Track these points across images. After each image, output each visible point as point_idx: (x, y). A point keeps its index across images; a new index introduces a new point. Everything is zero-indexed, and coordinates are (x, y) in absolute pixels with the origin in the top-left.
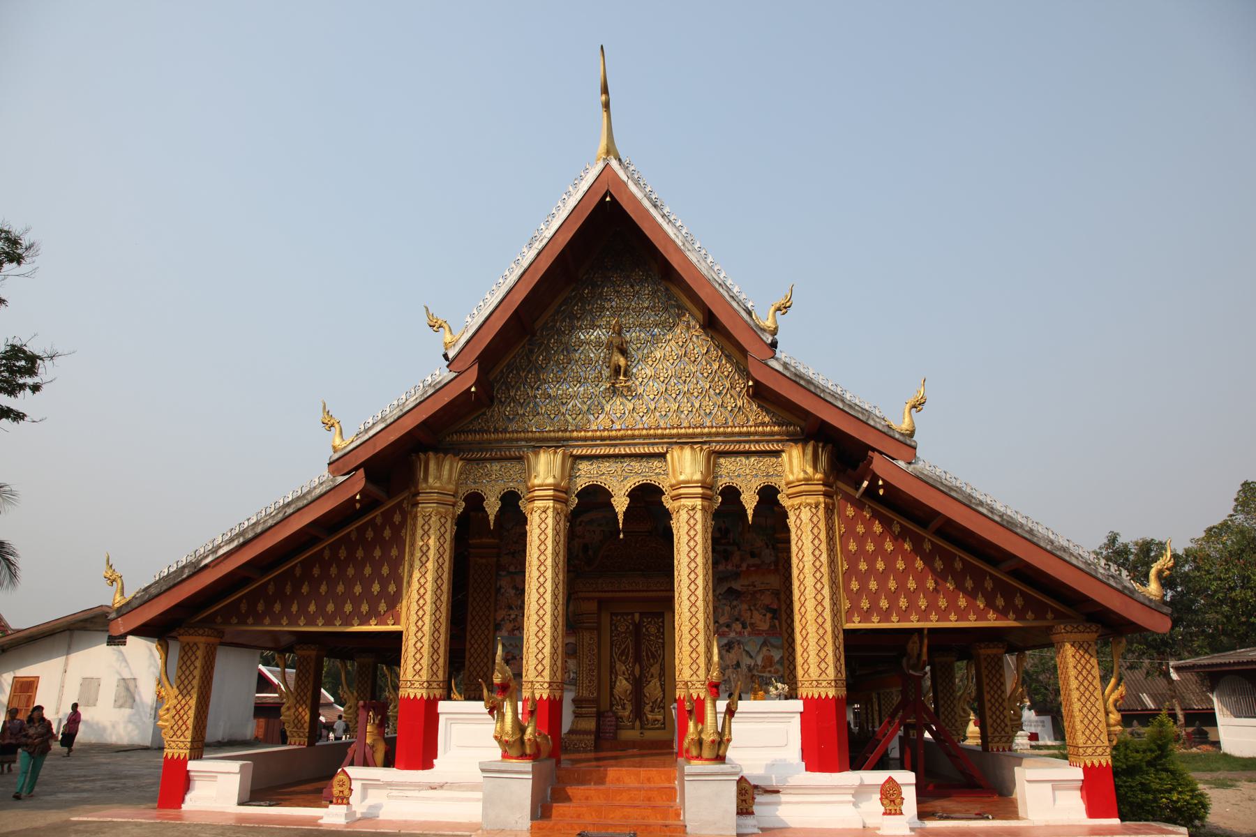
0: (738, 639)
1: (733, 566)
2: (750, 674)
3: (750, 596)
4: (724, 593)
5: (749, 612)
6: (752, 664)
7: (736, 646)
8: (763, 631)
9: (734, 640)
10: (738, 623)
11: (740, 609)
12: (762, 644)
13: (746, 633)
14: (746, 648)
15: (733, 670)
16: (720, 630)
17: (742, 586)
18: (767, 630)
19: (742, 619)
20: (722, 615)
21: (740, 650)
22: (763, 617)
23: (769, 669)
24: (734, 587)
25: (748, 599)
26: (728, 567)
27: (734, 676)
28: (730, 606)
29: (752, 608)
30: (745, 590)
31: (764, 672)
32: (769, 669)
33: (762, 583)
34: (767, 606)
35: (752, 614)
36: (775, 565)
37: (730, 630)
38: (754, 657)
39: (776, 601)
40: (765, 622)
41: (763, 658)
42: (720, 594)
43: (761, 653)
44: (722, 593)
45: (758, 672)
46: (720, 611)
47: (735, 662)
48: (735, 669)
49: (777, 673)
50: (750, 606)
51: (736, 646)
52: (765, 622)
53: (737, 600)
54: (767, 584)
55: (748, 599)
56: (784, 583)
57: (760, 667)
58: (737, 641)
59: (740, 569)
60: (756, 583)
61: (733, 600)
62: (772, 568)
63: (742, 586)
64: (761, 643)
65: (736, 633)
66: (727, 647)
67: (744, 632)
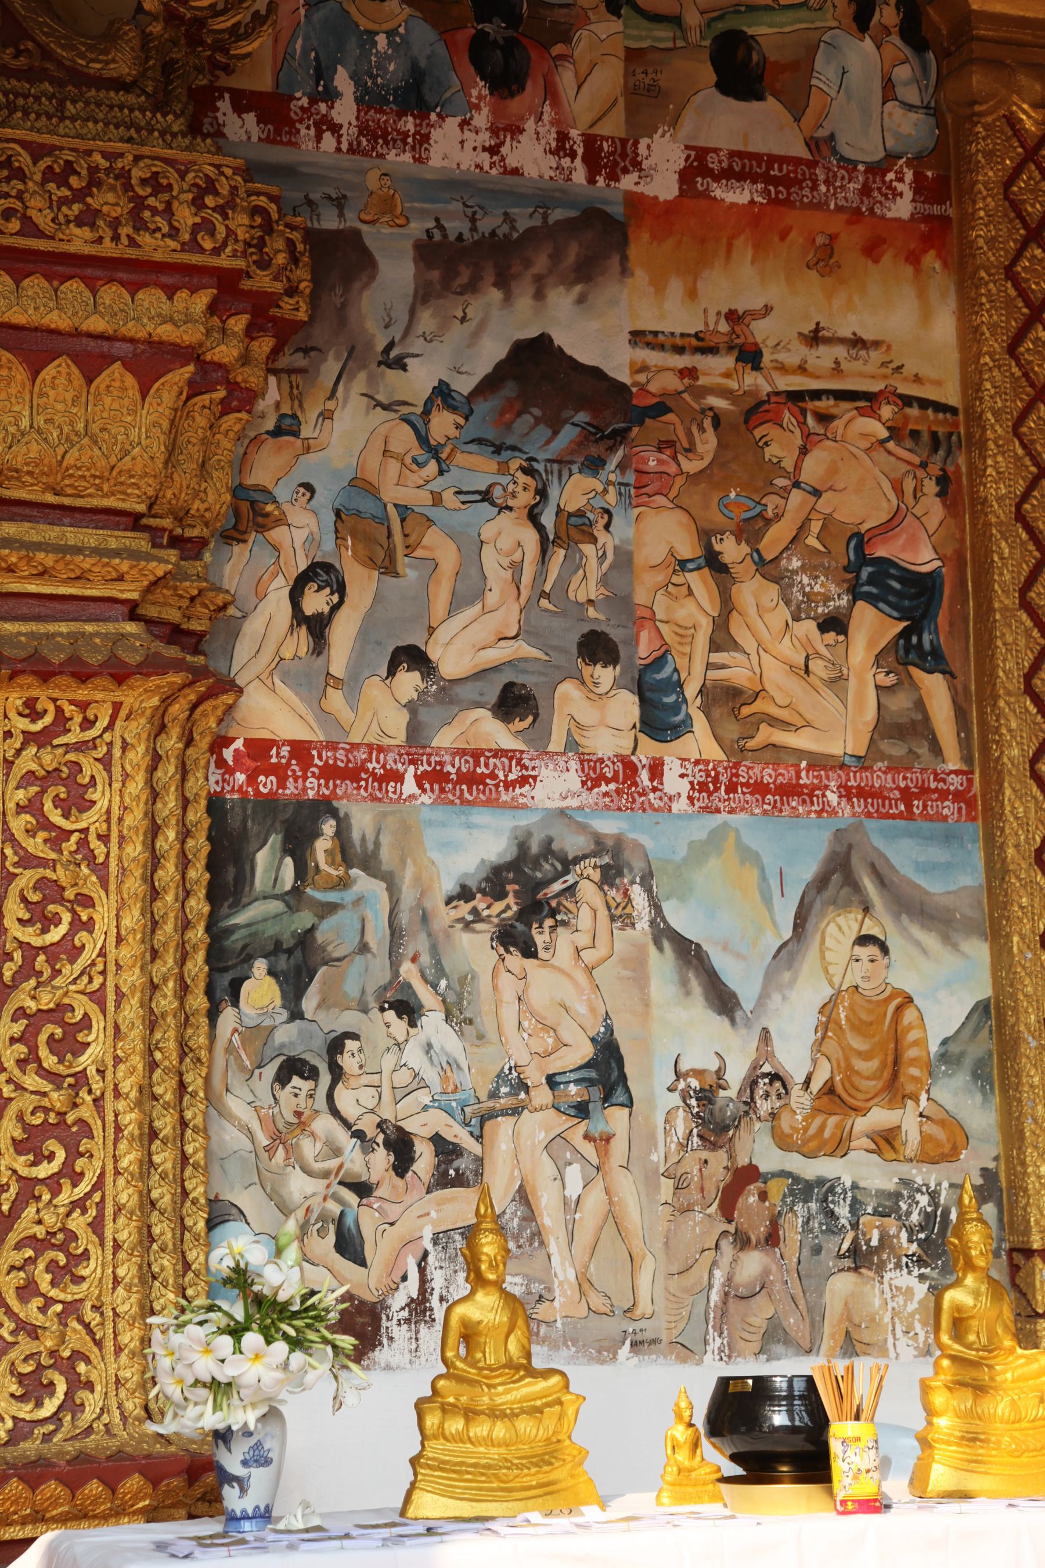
0: (608, 826)
1: (562, 147)
2: (719, 1160)
3: (708, 443)
4: (488, 385)
5: (699, 582)
6: (736, 1075)
7: (588, 891)
8: (819, 763)
9: (573, 843)
10: (605, 675)
11: (624, 560)
12: (821, 882)
13: (674, 782)
14: (677, 918)
15: (562, 1123)
16: (445, 739)
17: (637, 337)
18: (863, 763)
19: (645, 649)
20: (456, 605)
21: (624, 939)
22: (821, 642)
23: (879, 1117)
24: (560, 339)
25: (691, 466)
26: (516, 154)
27: (574, 1174)
28: (533, 517)
29: (730, 550)
30: (673, 383)
31: (840, 1147)
32: (879, 1117)
33: (815, 338)
34: (860, 540)
35: (727, 606)
36: (920, 187)
37: (539, 737)
38: (747, 996)
39: (933, 510)
40: (837, 682)
41: (828, 1009)
42: (442, 393)
43: (810, 960)
44: (464, 385)
45: (783, 1142)
46: (448, 557)
47: (585, 1051)
48: (582, 1110)
49: (951, 1155)
50: (705, 535)
51: (588, 891)
52: (837, 682)
53: (594, 466)
54: (857, 342)
55: (691, 466)
56: (1012, 349)
57: (800, 1101)
58: (600, 845)
59: (628, 182)
60: (761, 331)
61: (562, 461)
62: (903, 208)
63: (637, 337)
64: (808, 871)
65: (593, 780)
66: (509, 906)
67: (656, 769)
